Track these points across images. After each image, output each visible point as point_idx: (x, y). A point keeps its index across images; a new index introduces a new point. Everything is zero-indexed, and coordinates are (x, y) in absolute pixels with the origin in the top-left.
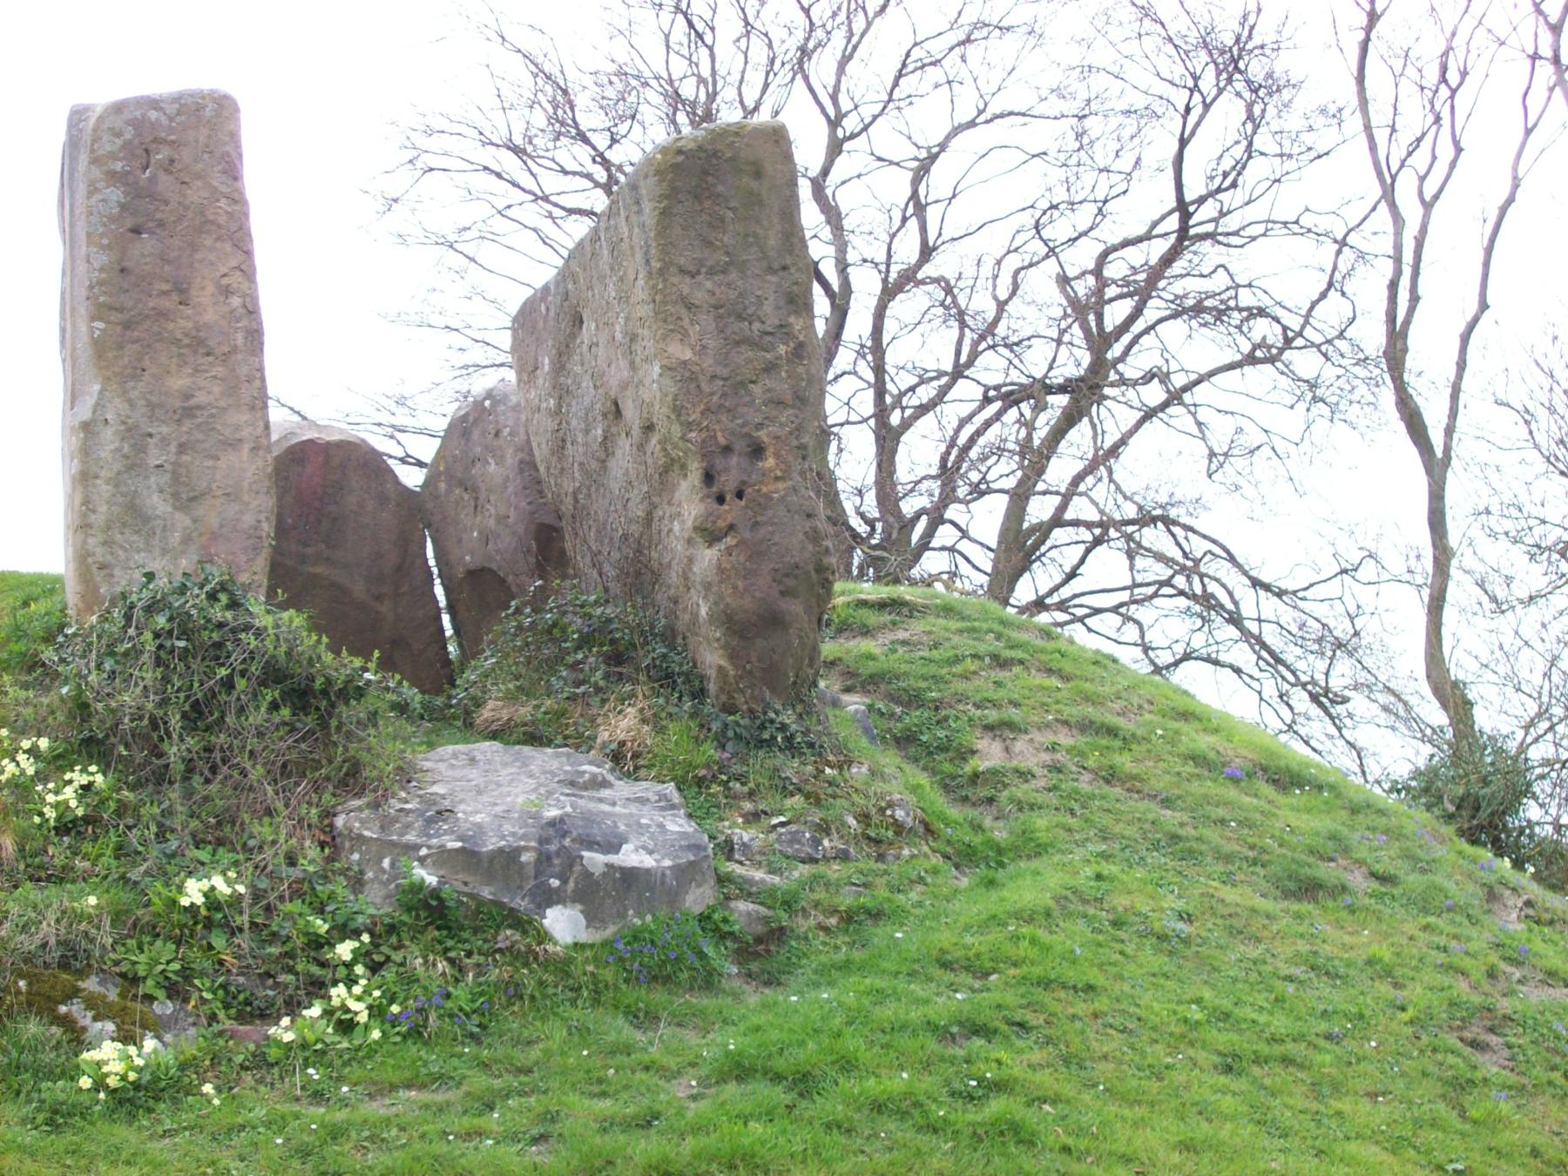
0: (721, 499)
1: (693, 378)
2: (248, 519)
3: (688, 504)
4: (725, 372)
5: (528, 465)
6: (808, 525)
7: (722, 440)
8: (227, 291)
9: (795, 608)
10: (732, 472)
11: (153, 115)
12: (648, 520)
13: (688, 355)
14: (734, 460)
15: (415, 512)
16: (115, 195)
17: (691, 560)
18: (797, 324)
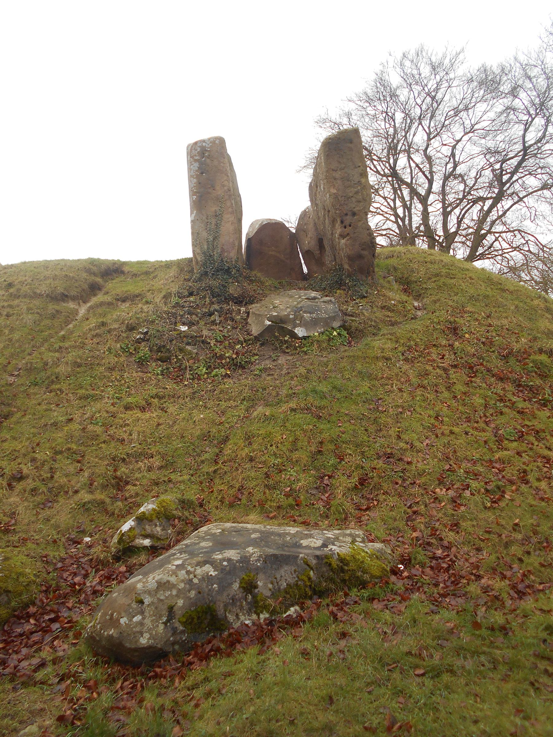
0: (345, 227)
2: (231, 240)
4: (345, 195)
6: (368, 232)
7: (345, 212)
9: (365, 253)
10: (348, 219)
11: (204, 144)
13: (335, 191)
14: (348, 217)
15: (294, 238)
16: (197, 165)
17: (339, 243)
18: (363, 180)
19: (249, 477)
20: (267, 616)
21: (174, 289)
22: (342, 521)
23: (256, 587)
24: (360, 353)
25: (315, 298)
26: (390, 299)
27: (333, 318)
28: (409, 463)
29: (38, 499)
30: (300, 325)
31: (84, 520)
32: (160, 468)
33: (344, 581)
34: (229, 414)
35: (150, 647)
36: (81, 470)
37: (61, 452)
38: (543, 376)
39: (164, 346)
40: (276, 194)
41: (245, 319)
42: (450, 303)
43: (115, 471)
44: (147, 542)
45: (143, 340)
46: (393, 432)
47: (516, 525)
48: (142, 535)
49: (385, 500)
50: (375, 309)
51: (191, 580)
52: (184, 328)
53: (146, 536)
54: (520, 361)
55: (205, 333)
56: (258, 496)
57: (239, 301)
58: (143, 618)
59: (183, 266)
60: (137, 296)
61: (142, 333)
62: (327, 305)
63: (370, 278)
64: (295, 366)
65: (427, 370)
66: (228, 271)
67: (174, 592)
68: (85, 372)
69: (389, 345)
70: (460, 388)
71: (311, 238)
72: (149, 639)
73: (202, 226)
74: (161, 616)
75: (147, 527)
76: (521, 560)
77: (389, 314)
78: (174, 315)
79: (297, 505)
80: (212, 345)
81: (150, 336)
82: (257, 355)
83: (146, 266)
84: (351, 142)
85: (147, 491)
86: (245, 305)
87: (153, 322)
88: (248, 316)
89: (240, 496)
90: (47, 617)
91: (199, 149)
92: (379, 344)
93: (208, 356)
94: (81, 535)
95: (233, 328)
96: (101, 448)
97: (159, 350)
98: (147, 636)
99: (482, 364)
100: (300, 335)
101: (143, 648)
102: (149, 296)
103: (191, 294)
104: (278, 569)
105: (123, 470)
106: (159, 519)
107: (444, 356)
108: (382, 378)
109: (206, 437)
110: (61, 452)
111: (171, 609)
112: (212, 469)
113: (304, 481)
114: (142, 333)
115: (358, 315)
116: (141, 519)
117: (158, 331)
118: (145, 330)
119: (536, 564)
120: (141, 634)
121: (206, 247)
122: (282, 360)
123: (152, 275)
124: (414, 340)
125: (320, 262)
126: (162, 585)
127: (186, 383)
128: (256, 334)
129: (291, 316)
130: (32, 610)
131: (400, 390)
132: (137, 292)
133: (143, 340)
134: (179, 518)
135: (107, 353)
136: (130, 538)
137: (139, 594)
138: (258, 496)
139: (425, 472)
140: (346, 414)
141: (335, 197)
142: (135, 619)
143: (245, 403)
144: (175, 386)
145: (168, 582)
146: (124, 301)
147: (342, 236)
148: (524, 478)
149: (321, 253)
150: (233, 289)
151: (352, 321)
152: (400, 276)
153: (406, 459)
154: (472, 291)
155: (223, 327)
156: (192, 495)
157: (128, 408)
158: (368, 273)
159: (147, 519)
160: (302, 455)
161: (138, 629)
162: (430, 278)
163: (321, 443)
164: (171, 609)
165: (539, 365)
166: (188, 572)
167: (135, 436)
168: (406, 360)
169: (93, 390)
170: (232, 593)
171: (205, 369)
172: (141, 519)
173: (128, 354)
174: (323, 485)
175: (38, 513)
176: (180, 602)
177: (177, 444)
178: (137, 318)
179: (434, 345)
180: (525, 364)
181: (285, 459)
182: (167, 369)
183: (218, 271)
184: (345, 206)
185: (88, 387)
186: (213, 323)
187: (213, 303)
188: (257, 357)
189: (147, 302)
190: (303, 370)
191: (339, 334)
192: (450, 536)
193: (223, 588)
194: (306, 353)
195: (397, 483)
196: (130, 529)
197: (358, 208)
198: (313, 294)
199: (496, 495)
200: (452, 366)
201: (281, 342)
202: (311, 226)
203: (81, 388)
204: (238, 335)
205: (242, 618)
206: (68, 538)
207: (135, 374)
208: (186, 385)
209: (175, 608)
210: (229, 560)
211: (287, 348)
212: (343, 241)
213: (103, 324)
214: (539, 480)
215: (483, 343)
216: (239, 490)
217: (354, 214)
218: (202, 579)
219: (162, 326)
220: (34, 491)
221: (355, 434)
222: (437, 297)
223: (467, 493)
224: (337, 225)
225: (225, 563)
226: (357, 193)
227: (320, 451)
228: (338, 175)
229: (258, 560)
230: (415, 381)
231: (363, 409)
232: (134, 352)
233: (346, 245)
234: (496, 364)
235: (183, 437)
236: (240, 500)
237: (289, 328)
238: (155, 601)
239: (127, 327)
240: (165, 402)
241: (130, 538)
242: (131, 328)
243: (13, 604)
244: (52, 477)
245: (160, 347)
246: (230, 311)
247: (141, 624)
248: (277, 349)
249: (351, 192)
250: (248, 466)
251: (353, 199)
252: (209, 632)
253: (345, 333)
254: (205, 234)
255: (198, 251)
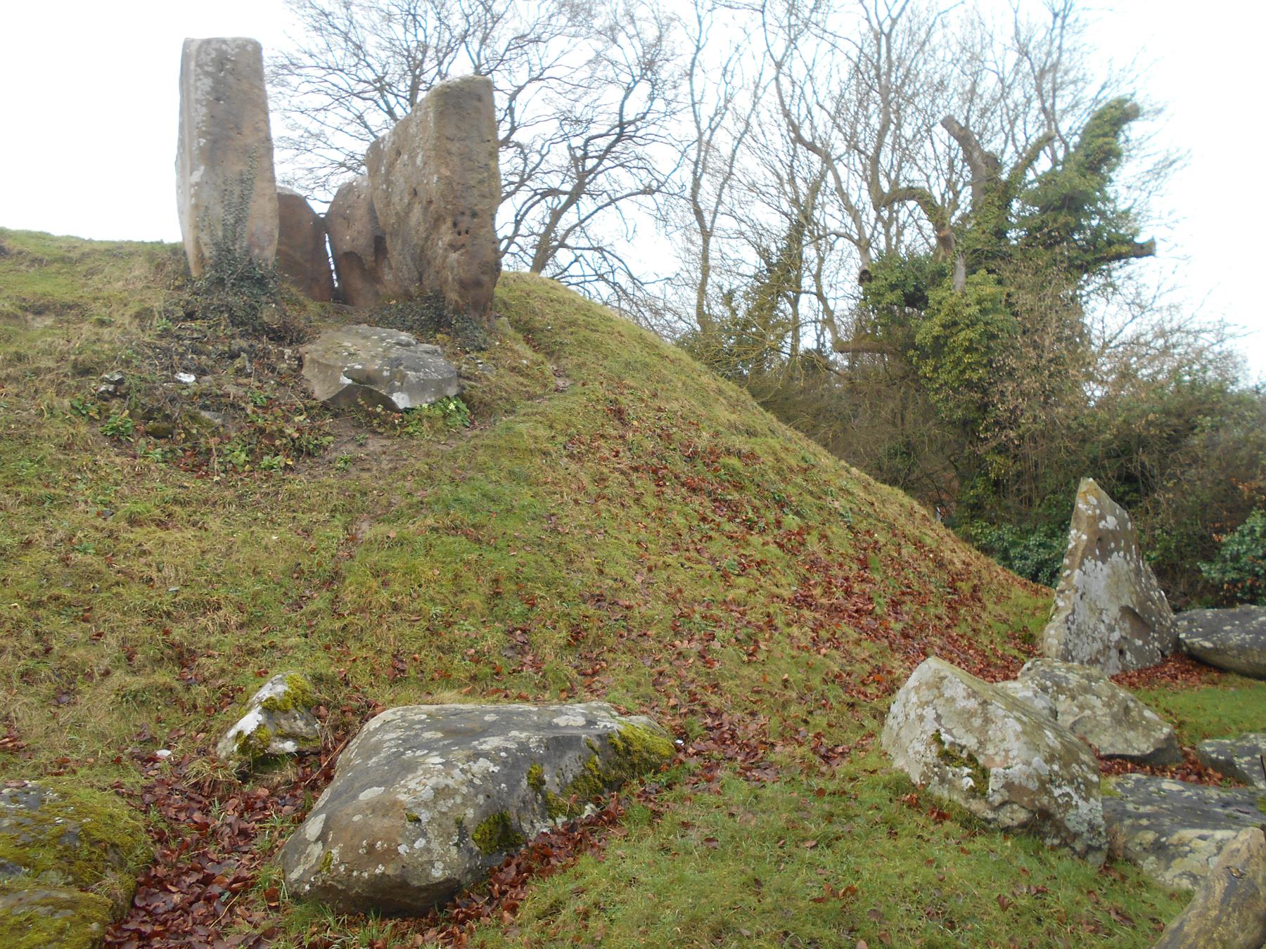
0: (459, 234)
1: (450, 183)
2: (268, 228)
3: (446, 235)
5: (372, 210)
8: (257, 130)
9: (485, 278)
10: (465, 222)
12: (427, 238)
13: (448, 174)
15: (321, 225)
17: (446, 257)
18: (492, 164)
19: (402, 635)
20: (565, 819)
21: (158, 305)
22: (570, 693)
23: (543, 783)
24: (502, 442)
25: (408, 344)
26: (520, 357)
27: (448, 382)
28: (628, 608)
29: (45, 689)
30: (400, 390)
31: (142, 718)
32: (241, 626)
33: (633, 766)
34: (319, 531)
35: (448, 880)
36: (100, 635)
37: (40, 604)
38: (739, 487)
39: (159, 409)
40: (318, 153)
41: (294, 371)
42: (601, 371)
43: (167, 633)
44: (289, 746)
45: (113, 395)
46: (589, 563)
47: (786, 680)
48: (278, 735)
49: (615, 660)
50: (502, 371)
51: (471, 781)
52: (189, 378)
53: (286, 737)
54: (708, 465)
55: (232, 390)
56: (431, 664)
57: (280, 335)
58: (429, 842)
59: (161, 260)
60: (70, 307)
61: (111, 383)
62: (433, 359)
63: (484, 318)
64: (399, 457)
65: (602, 473)
66: (261, 282)
67: (459, 800)
68: (16, 451)
69: (542, 432)
70: (649, 500)
71: (359, 232)
72: (444, 869)
73: (215, 194)
74: (450, 836)
75: (283, 721)
76: (806, 722)
77: (526, 382)
78: (166, 351)
79: (497, 674)
80: (249, 412)
81: (129, 388)
82: (329, 434)
83: (57, 244)
84: (480, 99)
85: (238, 665)
86: (290, 344)
87: (127, 362)
88: (301, 366)
89: (400, 666)
90: (189, 880)
91: (214, 55)
92: (526, 429)
93: (246, 432)
94: (150, 747)
95: (279, 384)
96: (118, 595)
97: (148, 416)
98: (439, 865)
99: (666, 468)
100: (401, 406)
101: (440, 883)
102: (99, 310)
103: (190, 316)
104: (561, 757)
105: (178, 633)
106: (296, 707)
107: (618, 452)
108: (546, 483)
109: (297, 571)
110: (40, 604)
111: (459, 823)
112: (338, 625)
113: (493, 638)
114: (111, 383)
115: (478, 379)
116: (270, 709)
117: (143, 380)
118: (117, 377)
119: (825, 725)
120: (431, 863)
121: (220, 234)
122: (375, 445)
123: (80, 268)
124: (575, 426)
125: (372, 276)
126: (441, 793)
127: (216, 478)
128: (324, 398)
129: (386, 374)
130: (161, 871)
131: (576, 502)
132: (68, 299)
133: (113, 395)
134: (327, 705)
135: (46, 416)
136: (262, 742)
137: (410, 810)
138: (431, 664)
139: (653, 619)
140: (516, 537)
141: (449, 182)
142: (417, 845)
143: (338, 515)
144: (199, 482)
145: (447, 786)
146: (39, 312)
147: (453, 247)
148: (771, 625)
149: (376, 261)
150: (269, 315)
151: (472, 387)
152: (517, 317)
153: (621, 602)
154: (625, 355)
155: (260, 381)
156: (324, 665)
157: (133, 521)
158: (484, 310)
159: (278, 709)
160: (476, 599)
161: (425, 858)
162: (563, 328)
163: (496, 581)
164: (459, 823)
165: (732, 471)
166: (462, 770)
167: (168, 572)
168: (571, 456)
169: (47, 486)
170: (522, 793)
171: (243, 455)
172: (270, 709)
173: (86, 419)
174: (520, 641)
175: (55, 716)
176: (470, 813)
177: (251, 585)
178: (95, 352)
179: (602, 436)
180: (716, 470)
181: (449, 605)
182: (171, 451)
183: (242, 280)
184: (462, 201)
185: (36, 481)
186: (240, 372)
187: (233, 337)
188: (331, 438)
189: (102, 323)
190: (421, 466)
191: (457, 407)
192: (715, 701)
193: (513, 787)
194: (411, 436)
195: (621, 636)
196: (259, 726)
197: (480, 207)
198: (404, 336)
199: (749, 645)
200: (631, 468)
201: (369, 414)
202: (361, 212)
203: (20, 482)
204: (290, 397)
205: (537, 825)
206: (131, 753)
207: (118, 460)
208: (217, 483)
209: (466, 822)
210: (506, 750)
211: (379, 425)
212: (454, 256)
213: (20, 358)
214: (789, 625)
215: (660, 436)
216: (394, 656)
217: (474, 215)
218: (484, 778)
219: (150, 370)
220: (26, 676)
221: (540, 567)
222: (581, 360)
223: (716, 645)
224: (444, 228)
225: (503, 754)
226: (481, 182)
227: (498, 593)
228: (455, 147)
229: (539, 747)
230: (592, 488)
231: (536, 530)
232: (97, 417)
233: (458, 262)
234: (682, 467)
235: (255, 572)
236: (403, 671)
237: (383, 392)
238: (437, 815)
239: (75, 366)
240: (195, 512)
241: (262, 742)
242: (84, 371)
243: (130, 864)
244: (48, 651)
245: (151, 411)
246: (267, 354)
247: (428, 850)
248: (360, 426)
249: (473, 178)
250: (395, 617)
251: (476, 192)
252: (500, 852)
253: (463, 406)
254: (219, 211)
255: (205, 238)
